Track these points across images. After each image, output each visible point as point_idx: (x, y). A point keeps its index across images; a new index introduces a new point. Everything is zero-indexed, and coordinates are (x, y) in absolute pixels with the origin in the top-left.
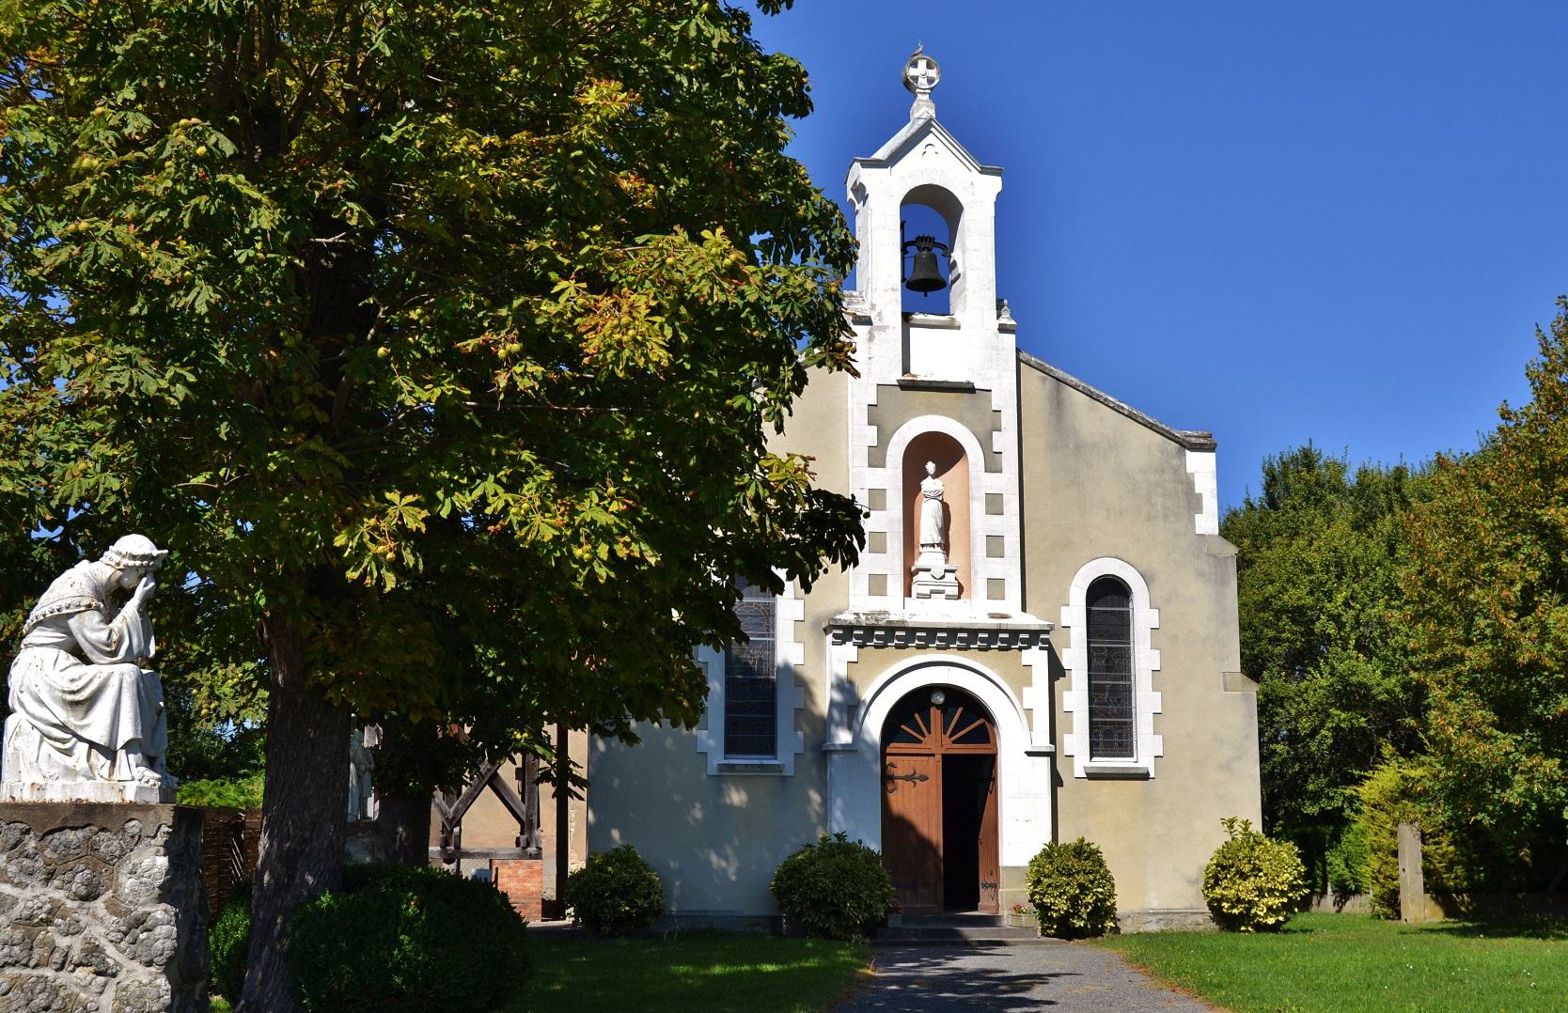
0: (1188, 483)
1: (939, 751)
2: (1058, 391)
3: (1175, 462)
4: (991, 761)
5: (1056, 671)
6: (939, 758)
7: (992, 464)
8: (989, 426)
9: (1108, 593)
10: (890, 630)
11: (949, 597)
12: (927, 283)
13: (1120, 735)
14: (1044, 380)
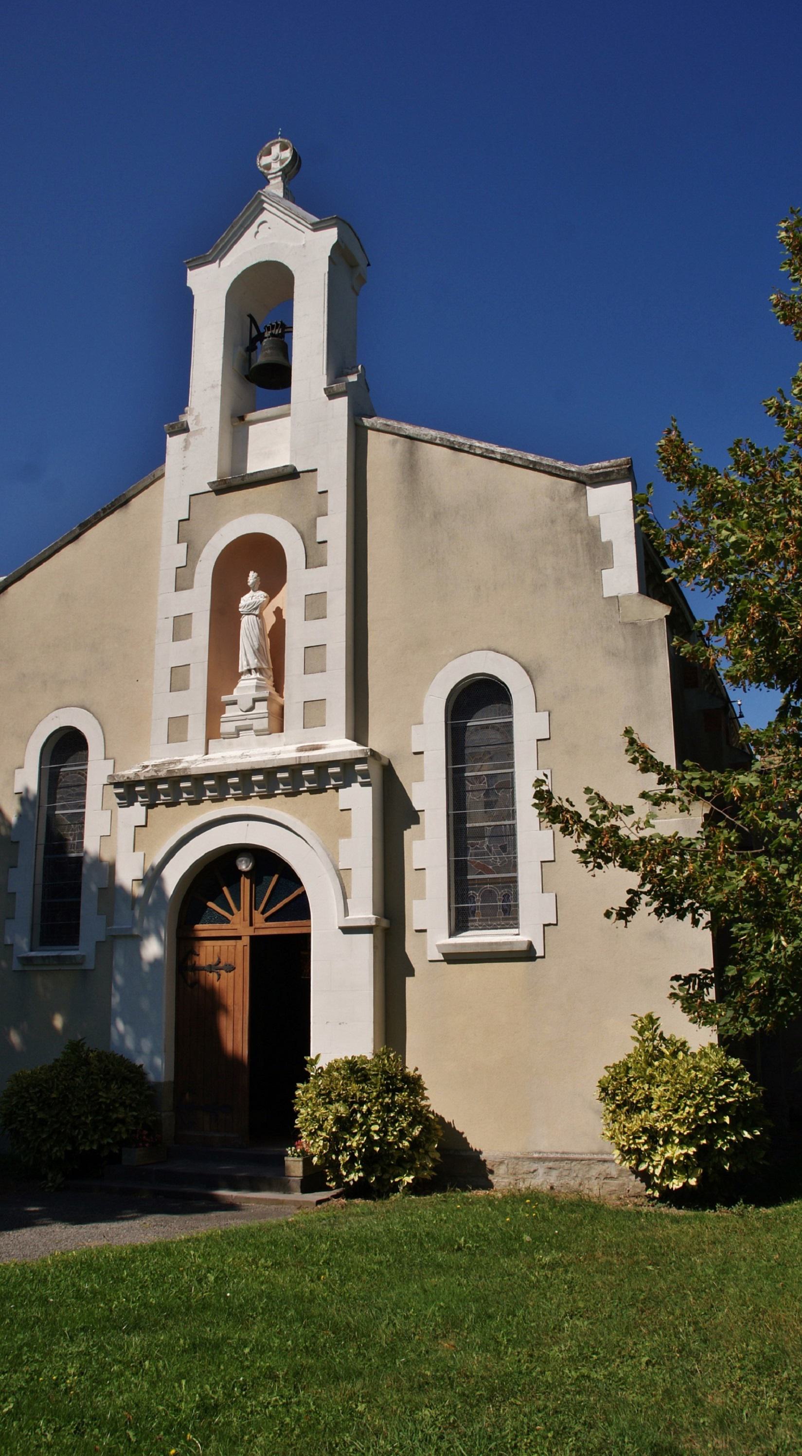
0: (592, 531)
1: (247, 932)
2: (411, 454)
3: (572, 505)
4: (303, 941)
5: (395, 814)
6: (246, 941)
7: (315, 556)
8: (314, 513)
9: (478, 701)
10: (174, 780)
11: (259, 733)
12: (262, 375)
13: (506, 897)
14: (394, 443)
